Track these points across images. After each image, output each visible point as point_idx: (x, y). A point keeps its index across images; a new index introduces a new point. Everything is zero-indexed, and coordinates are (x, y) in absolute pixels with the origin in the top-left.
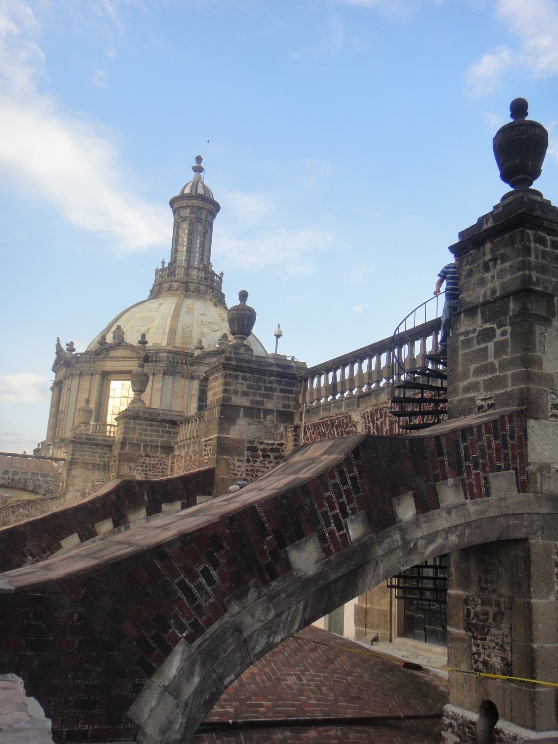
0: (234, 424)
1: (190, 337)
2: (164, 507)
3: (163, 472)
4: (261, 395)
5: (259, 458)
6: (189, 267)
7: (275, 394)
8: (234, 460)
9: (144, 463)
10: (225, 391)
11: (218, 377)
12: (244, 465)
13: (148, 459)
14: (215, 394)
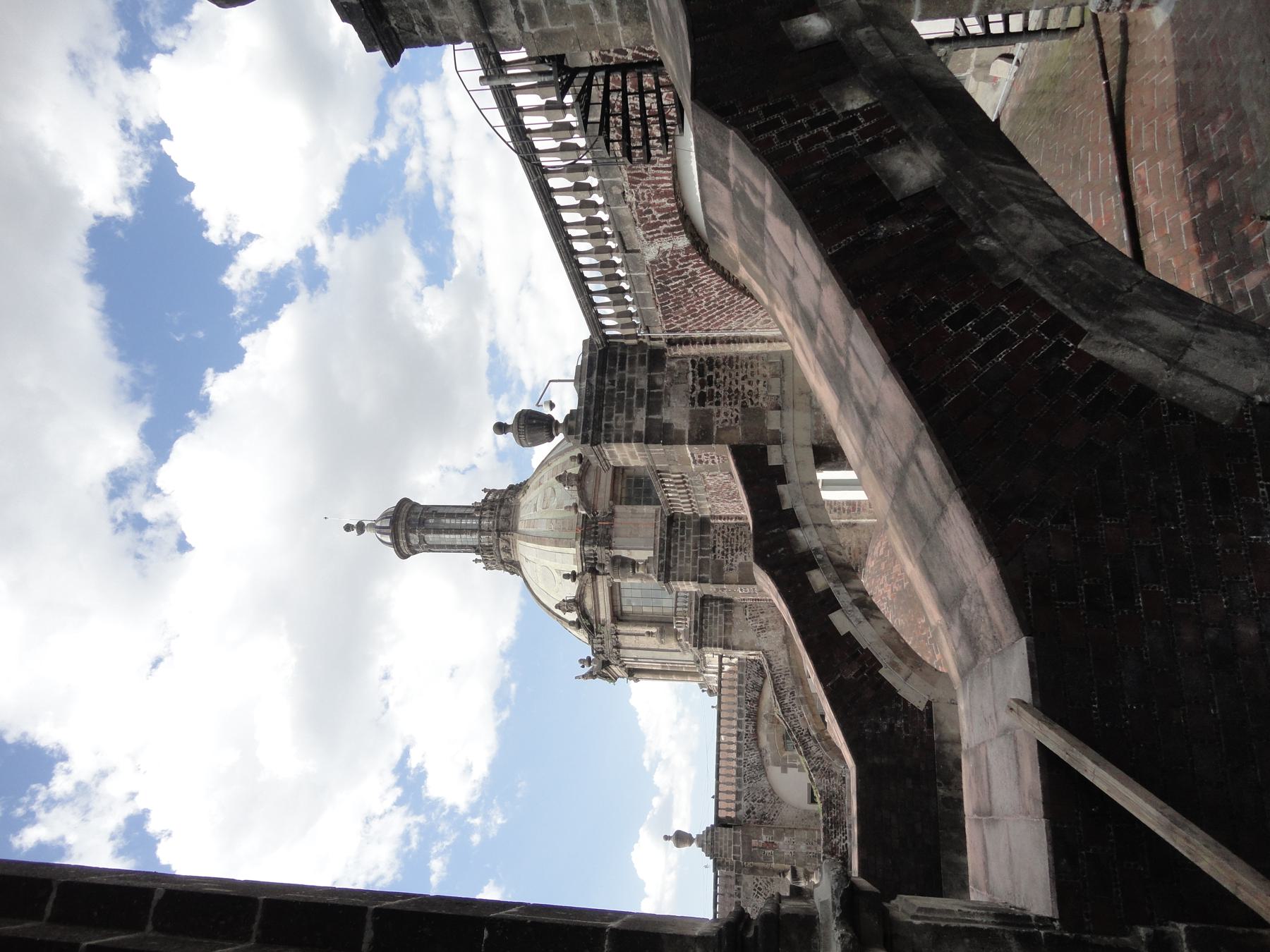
2: (786, 507)
3: (733, 530)
4: (631, 394)
5: (713, 390)
6: (480, 531)
8: (718, 421)
9: (723, 553)
10: (628, 440)
11: (609, 452)
12: (723, 408)
13: (717, 549)
14: (633, 455)
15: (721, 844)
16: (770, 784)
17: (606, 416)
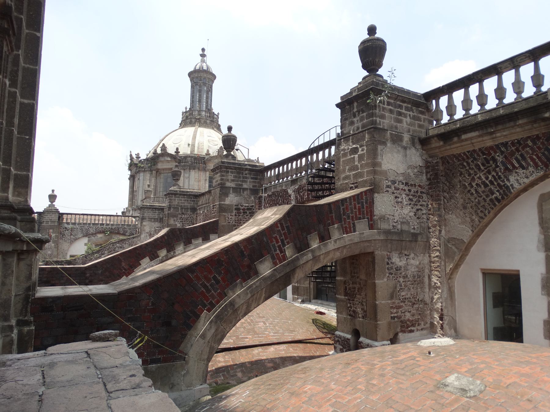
0: (228, 197)
1: (203, 149)
2: (193, 241)
3: (191, 222)
5: (241, 214)
7: (248, 180)
9: (181, 217)
10: (222, 179)
11: (218, 172)
12: (233, 218)
13: (183, 215)
14: (217, 181)
15: (50, 216)
16: (79, 238)
17: (232, 171)
